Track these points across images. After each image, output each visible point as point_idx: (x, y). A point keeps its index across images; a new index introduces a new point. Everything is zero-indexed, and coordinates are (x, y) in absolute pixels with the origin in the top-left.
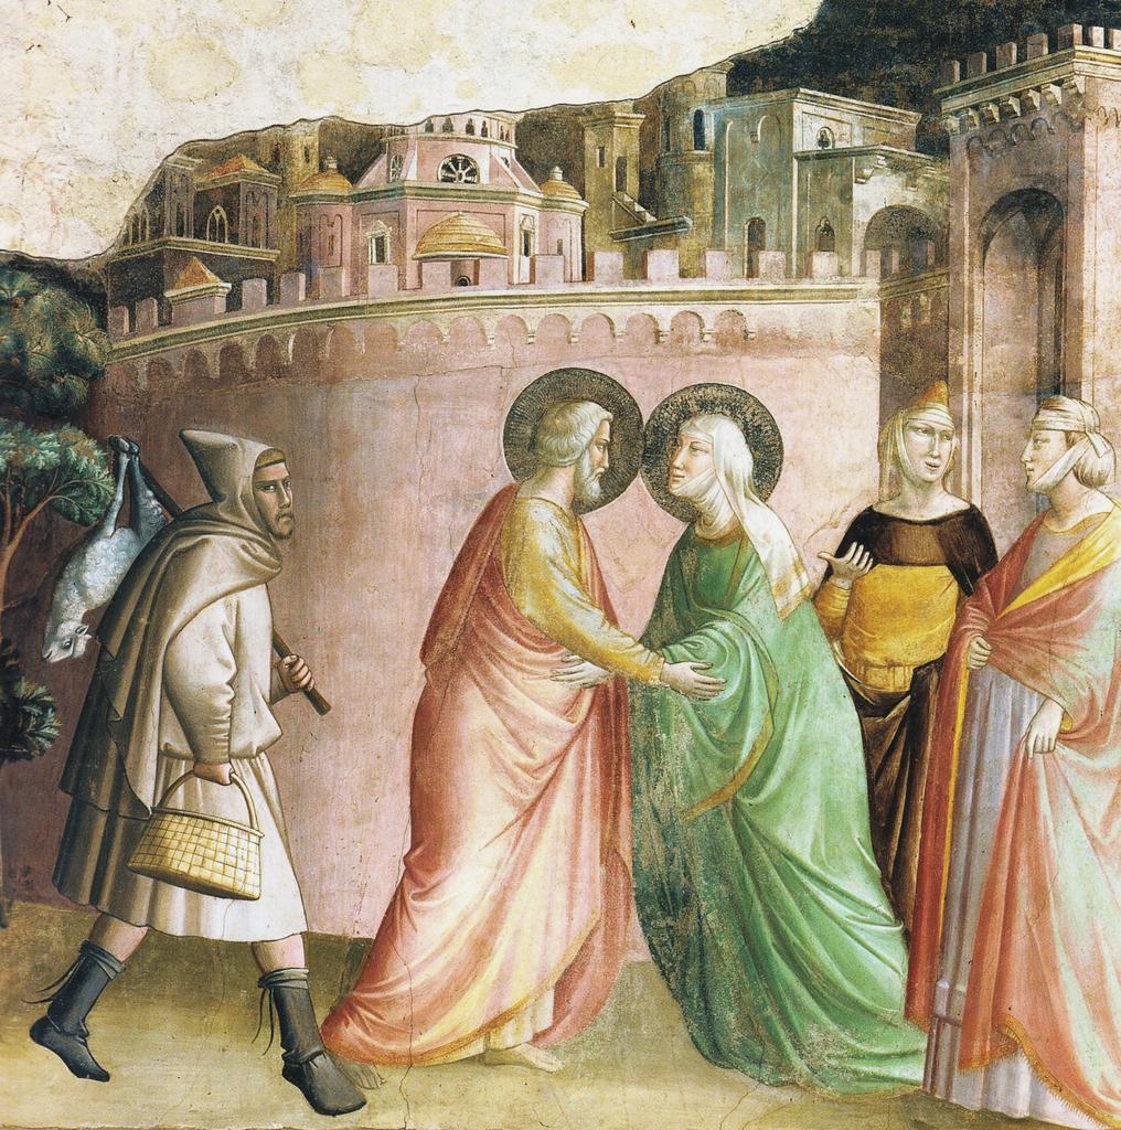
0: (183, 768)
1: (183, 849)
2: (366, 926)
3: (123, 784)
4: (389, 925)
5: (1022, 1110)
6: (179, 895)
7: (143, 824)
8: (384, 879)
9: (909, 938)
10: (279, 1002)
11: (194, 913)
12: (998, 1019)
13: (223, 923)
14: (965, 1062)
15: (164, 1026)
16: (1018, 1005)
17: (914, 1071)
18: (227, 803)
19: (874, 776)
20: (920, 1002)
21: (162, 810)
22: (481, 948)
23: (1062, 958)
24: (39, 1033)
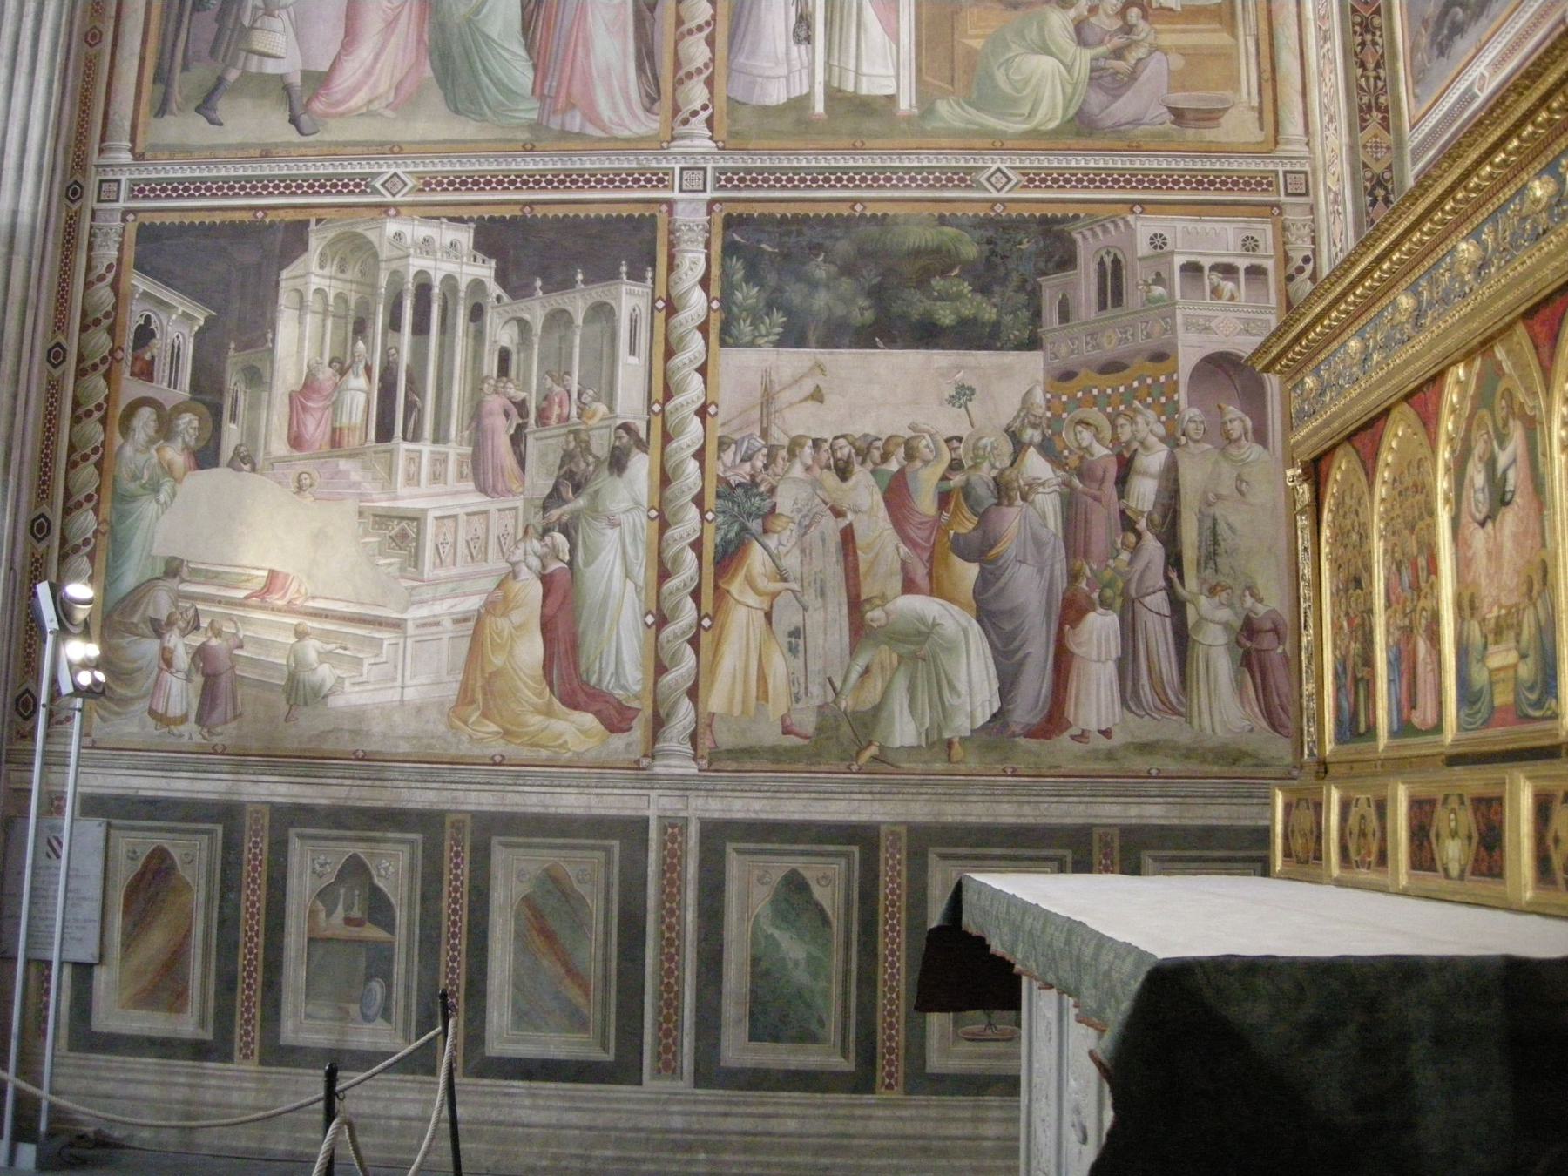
0: (260, 13)
1: (260, 42)
2: (324, 67)
3: (238, 19)
4: (333, 66)
5: (576, 129)
6: (255, 58)
7: (245, 33)
8: (334, 49)
9: (535, 67)
10: (290, 96)
11: (261, 64)
12: (569, 95)
13: (271, 67)
14: (554, 112)
15: (247, 104)
16: (577, 89)
17: (534, 116)
18: (277, 24)
19: (523, 9)
20: (538, 91)
21: (252, 28)
22: (369, 73)
23: (595, 74)
24: (198, 110)
